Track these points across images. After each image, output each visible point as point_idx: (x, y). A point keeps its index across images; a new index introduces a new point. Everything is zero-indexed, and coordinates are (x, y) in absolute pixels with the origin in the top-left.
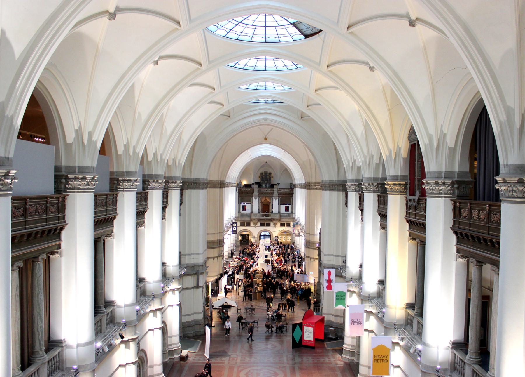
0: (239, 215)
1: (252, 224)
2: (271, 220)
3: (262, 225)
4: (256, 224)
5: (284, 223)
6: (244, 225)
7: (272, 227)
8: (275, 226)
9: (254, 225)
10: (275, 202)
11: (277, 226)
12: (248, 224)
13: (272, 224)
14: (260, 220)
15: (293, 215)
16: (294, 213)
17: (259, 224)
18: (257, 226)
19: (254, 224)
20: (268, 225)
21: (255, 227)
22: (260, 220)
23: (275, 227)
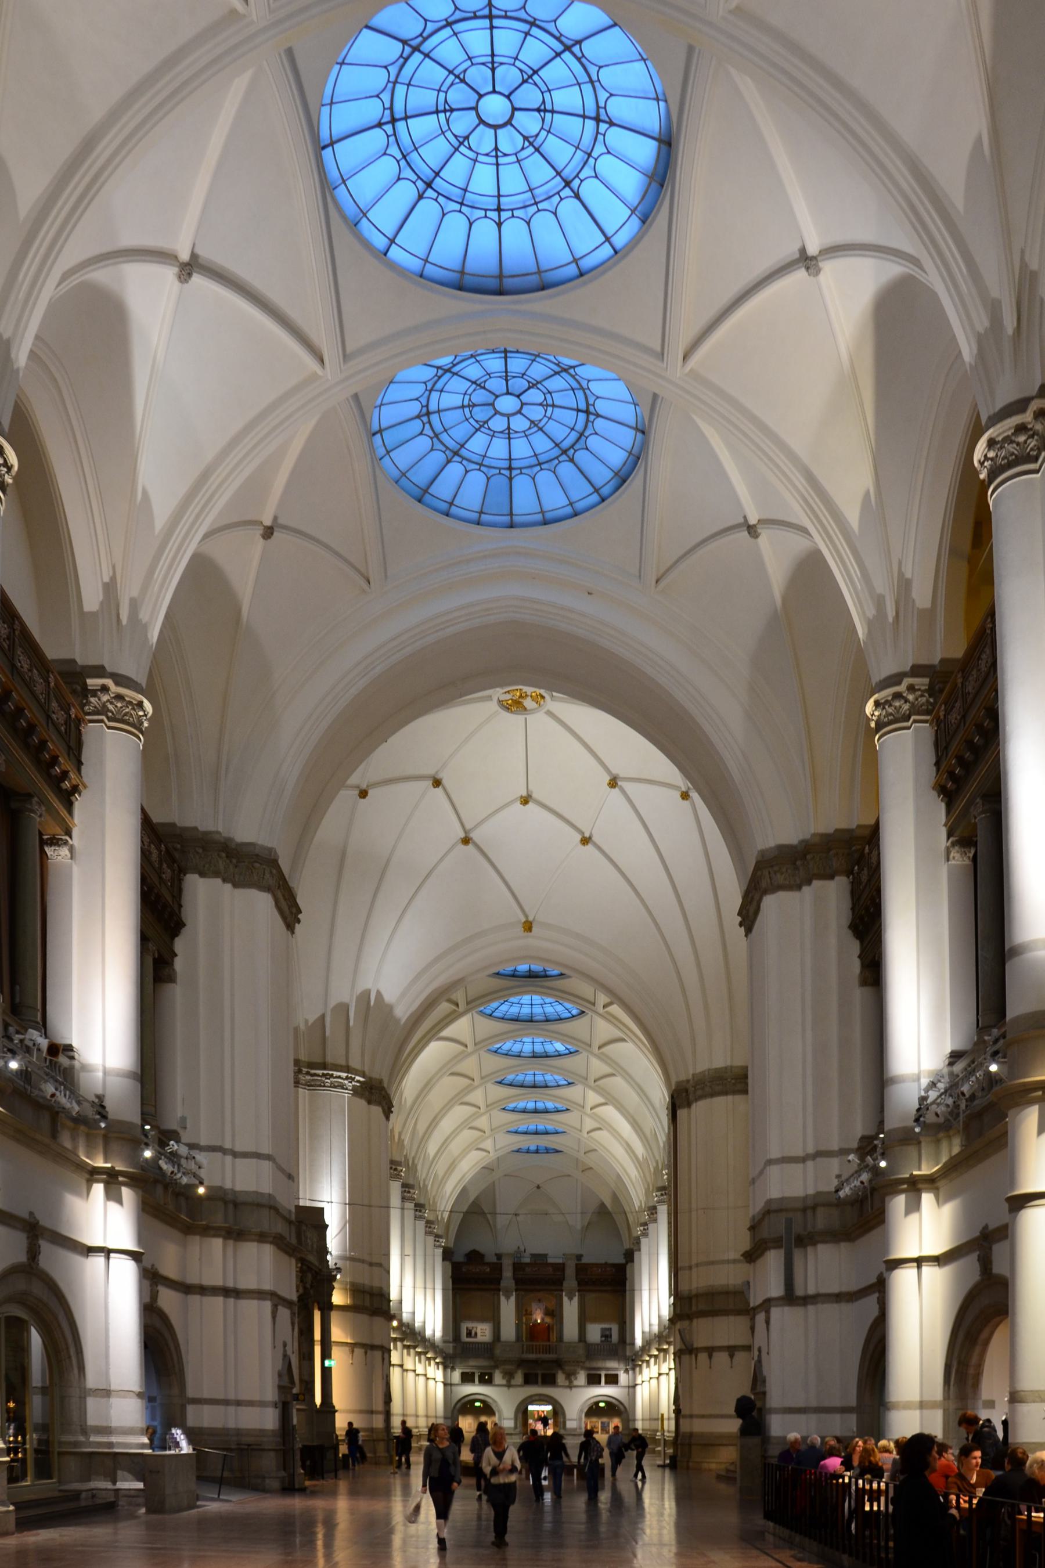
0: (455, 1348)
1: (498, 1378)
2: (559, 1364)
3: (528, 1380)
4: (509, 1376)
5: (600, 1376)
6: (473, 1381)
7: (561, 1386)
8: (571, 1382)
9: (504, 1382)
10: (571, 1309)
11: (576, 1383)
12: (486, 1379)
13: (561, 1378)
14: (521, 1363)
15: (628, 1347)
16: (628, 1341)
17: (519, 1378)
18: (513, 1382)
19: (503, 1378)
20: (550, 1380)
21: (509, 1385)
22: (521, 1363)
23: (571, 1387)
